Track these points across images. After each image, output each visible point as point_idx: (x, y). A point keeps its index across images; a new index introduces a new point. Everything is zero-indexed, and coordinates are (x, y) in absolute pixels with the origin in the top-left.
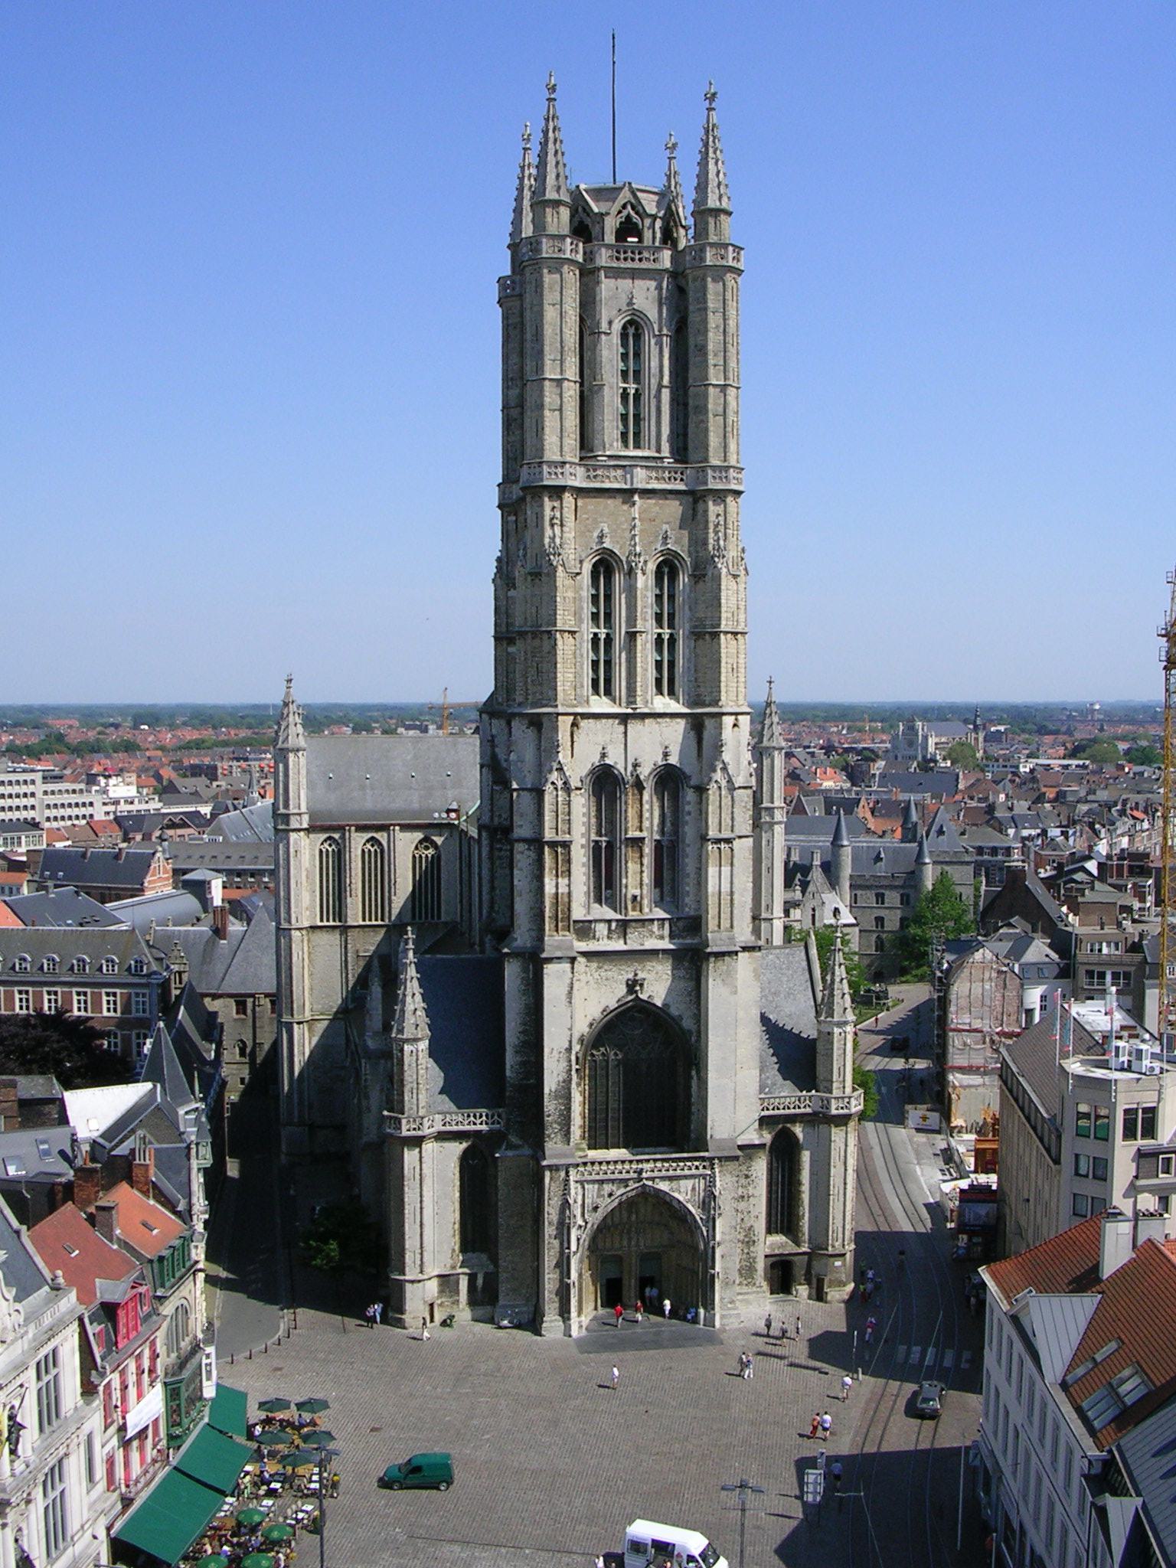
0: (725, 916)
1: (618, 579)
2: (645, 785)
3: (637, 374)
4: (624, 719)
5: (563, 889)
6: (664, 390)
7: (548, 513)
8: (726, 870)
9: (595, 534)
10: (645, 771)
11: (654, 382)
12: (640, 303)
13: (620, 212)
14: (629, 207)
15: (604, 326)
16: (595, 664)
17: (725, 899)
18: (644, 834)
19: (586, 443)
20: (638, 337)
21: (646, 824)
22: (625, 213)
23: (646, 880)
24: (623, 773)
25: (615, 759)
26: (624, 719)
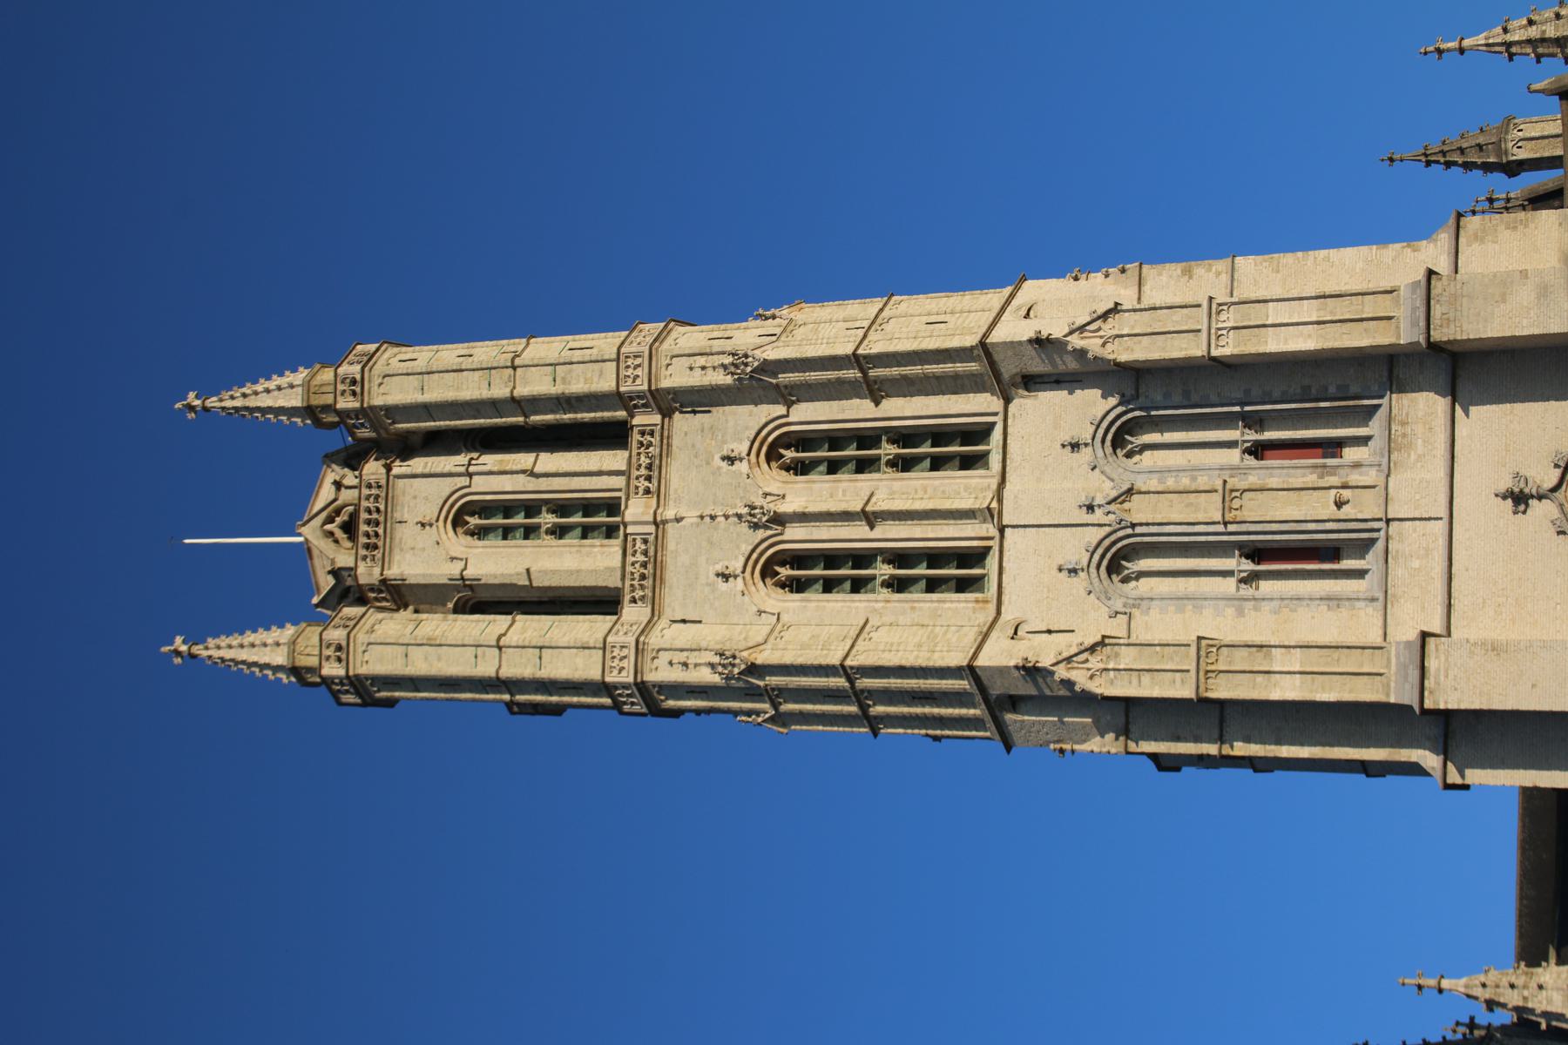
0: (1370, 307)
1: (797, 536)
2: (1125, 487)
3: (531, 508)
4: (1002, 530)
5: (1295, 661)
6: (538, 469)
7: (676, 675)
8: (1275, 313)
9: (722, 585)
10: (1104, 489)
11: (532, 484)
12: (430, 512)
13: (336, 541)
14: (329, 527)
15: (455, 569)
16: (933, 585)
17: (1343, 309)
18: (1218, 484)
19: (602, 602)
20: (484, 509)
21: (1203, 481)
22: (339, 534)
23: (1311, 479)
24: (1108, 529)
25: (1077, 546)
26: (1002, 530)
